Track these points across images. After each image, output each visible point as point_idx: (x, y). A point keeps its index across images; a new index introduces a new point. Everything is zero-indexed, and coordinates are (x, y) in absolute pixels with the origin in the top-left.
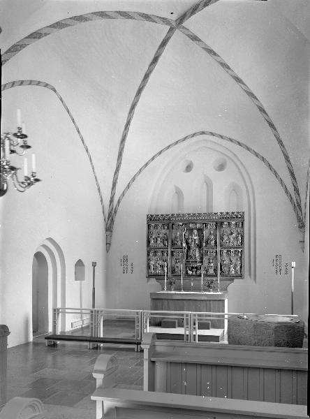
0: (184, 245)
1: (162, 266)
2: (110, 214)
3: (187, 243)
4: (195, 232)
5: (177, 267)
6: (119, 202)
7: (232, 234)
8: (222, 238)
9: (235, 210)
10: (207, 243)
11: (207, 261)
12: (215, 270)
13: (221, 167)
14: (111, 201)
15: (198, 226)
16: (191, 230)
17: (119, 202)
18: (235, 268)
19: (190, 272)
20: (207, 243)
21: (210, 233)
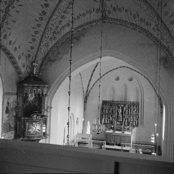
0: (116, 113)
1: (107, 120)
2: (86, 97)
3: (117, 112)
4: (121, 108)
5: (113, 121)
6: (89, 92)
7: (134, 110)
8: (131, 111)
9: (136, 101)
10: (125, 112)
11: (125, 120)
12: (128, 123)
13: (131, 80)
14: (87, 92)
15: (122, 106)
16: (119, 108)
17: (89, 92)
18: (135, 123)
19: (118, 123)
20: (125, 112)
21: (126, 109)
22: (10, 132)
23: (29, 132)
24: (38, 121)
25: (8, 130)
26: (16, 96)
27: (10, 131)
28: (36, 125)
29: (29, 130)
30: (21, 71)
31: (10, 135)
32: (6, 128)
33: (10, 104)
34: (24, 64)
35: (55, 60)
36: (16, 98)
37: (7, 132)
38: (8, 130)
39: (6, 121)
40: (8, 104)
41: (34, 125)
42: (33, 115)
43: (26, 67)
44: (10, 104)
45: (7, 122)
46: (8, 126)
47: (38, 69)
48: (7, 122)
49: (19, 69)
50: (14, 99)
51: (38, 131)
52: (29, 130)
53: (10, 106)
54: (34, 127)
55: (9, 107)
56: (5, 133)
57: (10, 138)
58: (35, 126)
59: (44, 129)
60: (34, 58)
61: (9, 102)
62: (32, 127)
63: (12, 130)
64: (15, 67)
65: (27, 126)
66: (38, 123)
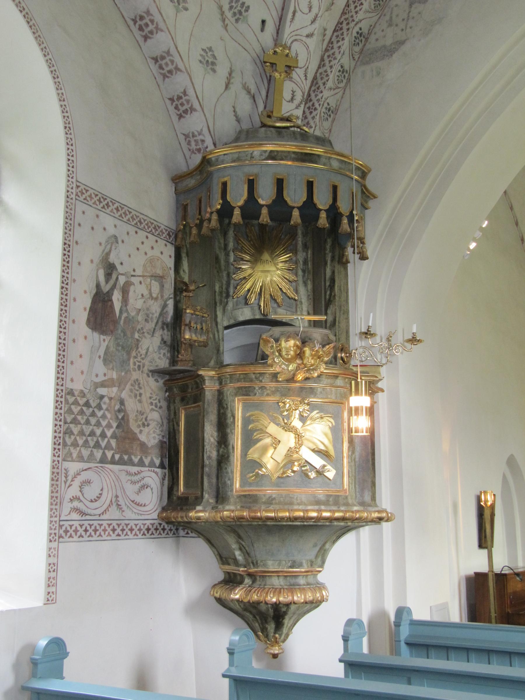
22: (134, 469)
23: (257, 464)
24: (312, 391)
25: (108, 447)
26: (170, 250)
27: (122, 462)
28: (303, 419)
29: (253, 454)
30: (191, 92)
31: (131, 489)
32: (92, 434)
33: (122, 280)
34: (210, 49)
35: (402, 43)
36: (171, 263)
37: (103, 460)
38: (108, 447)
39: (97, 385)
40: (108, 276)
41: (289, 417)
42: (277, 340)
43: (222, 71)
44: (122, 280)
45: (102, 391)
46: (109, 426)
47: (299, 97)
48: (102, 391)
49: (177, 69)
50: (151, 261)
51: (317, 462)
52: (253, 454)
53: (125, 292)
54: (287, 428)
55: (116, 298)
56: (81, 458)
57: (129, 514)
58: (296, 423)
59: (357, 411)
60: (270, 27)
61: (112, 259)
62: (272, 428)
63: (141, 463)
64: (156, 60)
65: (239, 423)
66: (313, 407)
